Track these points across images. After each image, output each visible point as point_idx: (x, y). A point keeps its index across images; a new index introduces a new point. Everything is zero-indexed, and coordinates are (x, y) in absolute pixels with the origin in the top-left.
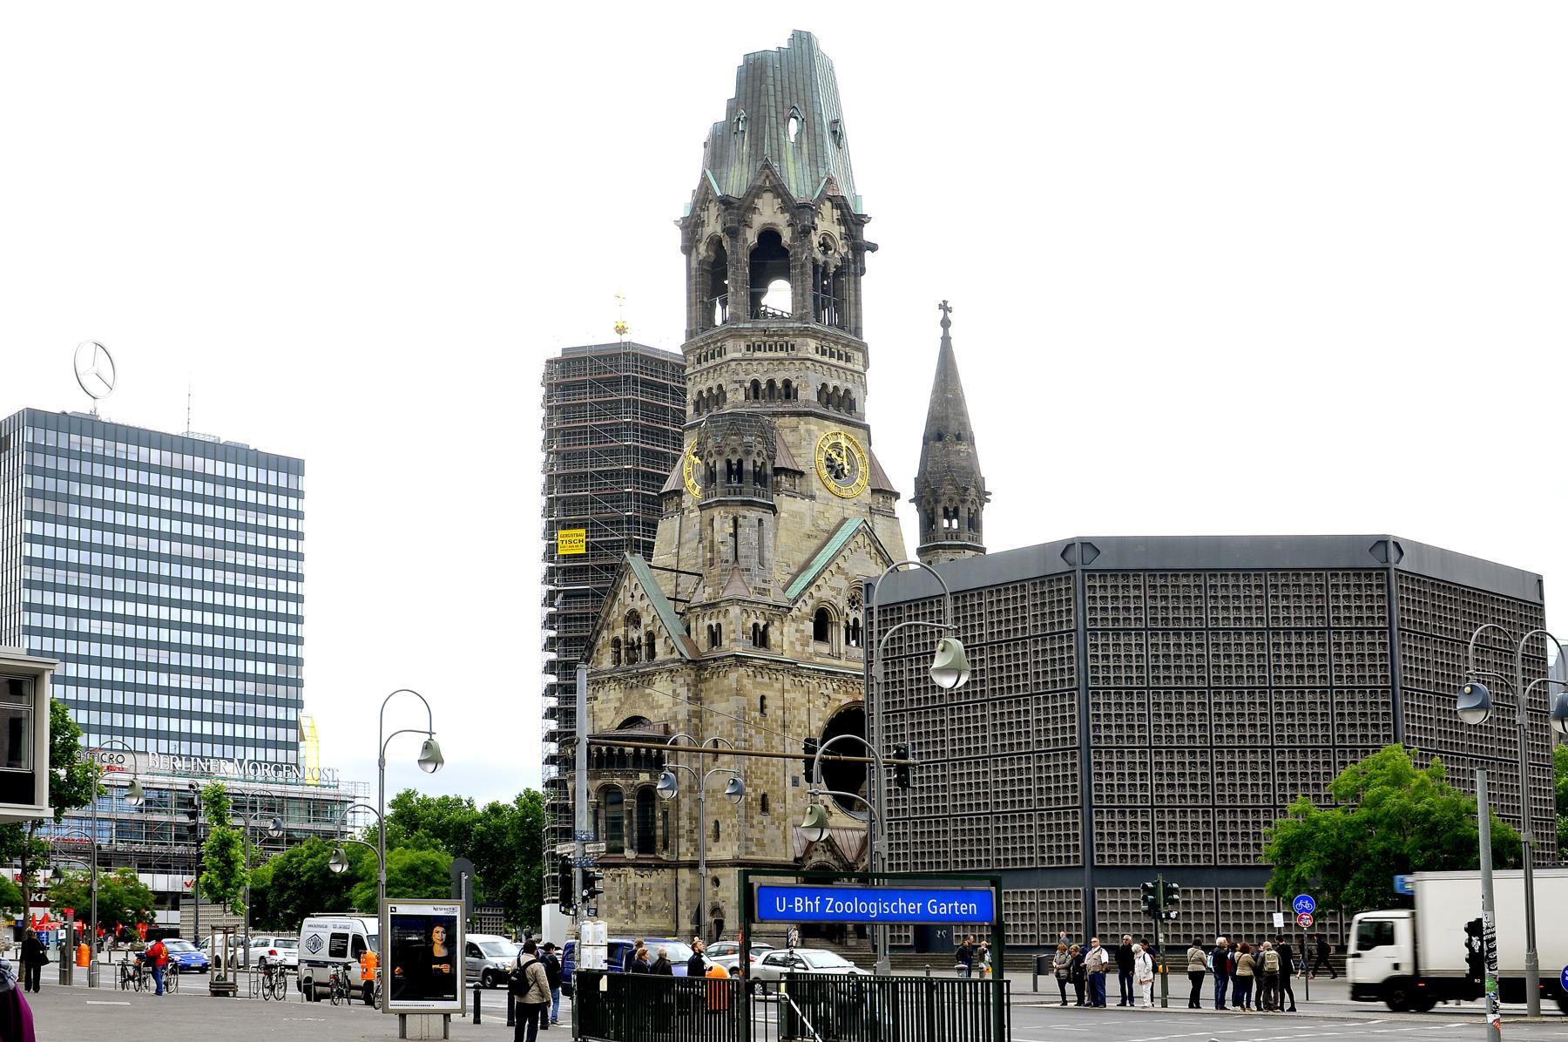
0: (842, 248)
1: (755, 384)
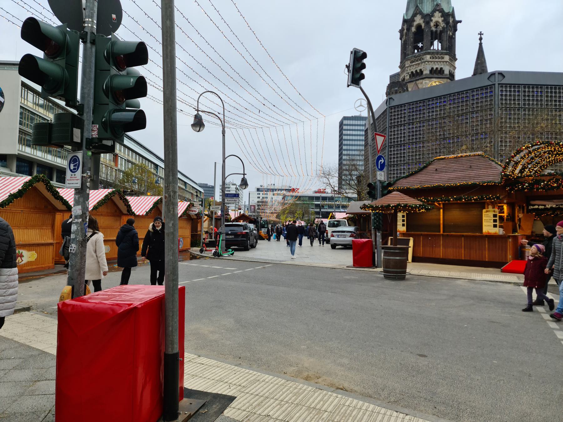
0: (442, 25)
1: (412, 72)
